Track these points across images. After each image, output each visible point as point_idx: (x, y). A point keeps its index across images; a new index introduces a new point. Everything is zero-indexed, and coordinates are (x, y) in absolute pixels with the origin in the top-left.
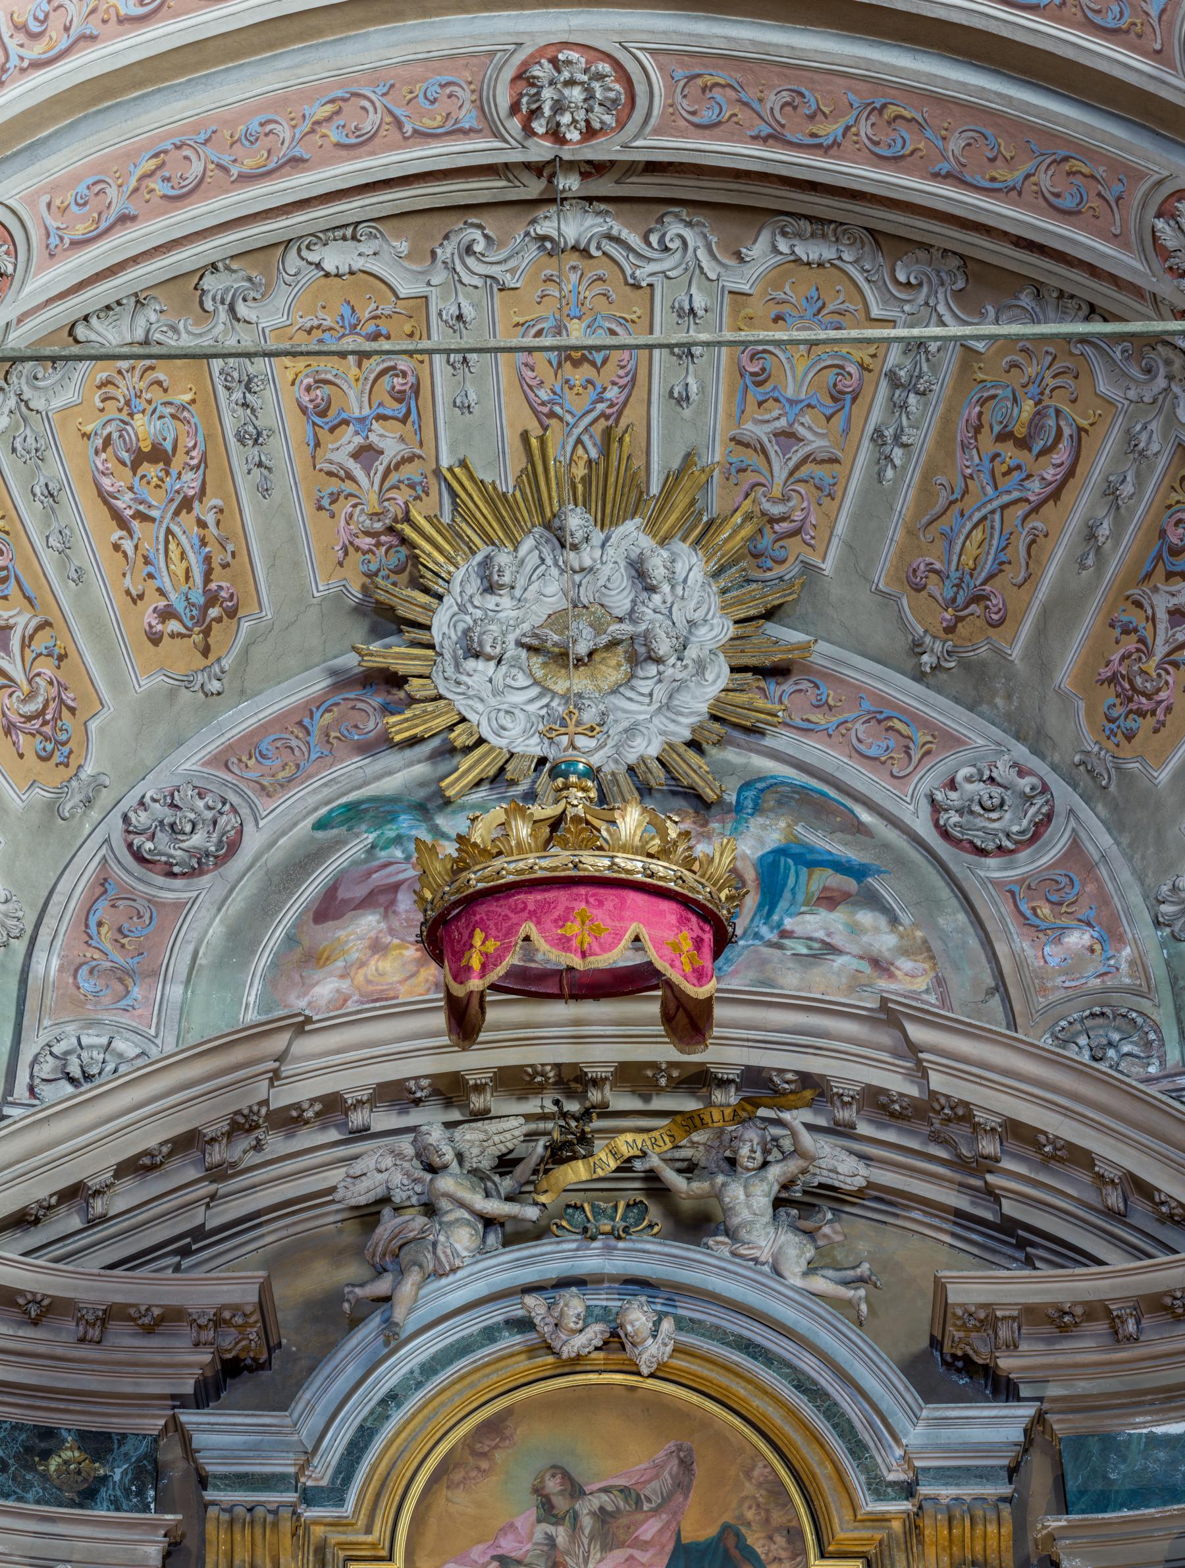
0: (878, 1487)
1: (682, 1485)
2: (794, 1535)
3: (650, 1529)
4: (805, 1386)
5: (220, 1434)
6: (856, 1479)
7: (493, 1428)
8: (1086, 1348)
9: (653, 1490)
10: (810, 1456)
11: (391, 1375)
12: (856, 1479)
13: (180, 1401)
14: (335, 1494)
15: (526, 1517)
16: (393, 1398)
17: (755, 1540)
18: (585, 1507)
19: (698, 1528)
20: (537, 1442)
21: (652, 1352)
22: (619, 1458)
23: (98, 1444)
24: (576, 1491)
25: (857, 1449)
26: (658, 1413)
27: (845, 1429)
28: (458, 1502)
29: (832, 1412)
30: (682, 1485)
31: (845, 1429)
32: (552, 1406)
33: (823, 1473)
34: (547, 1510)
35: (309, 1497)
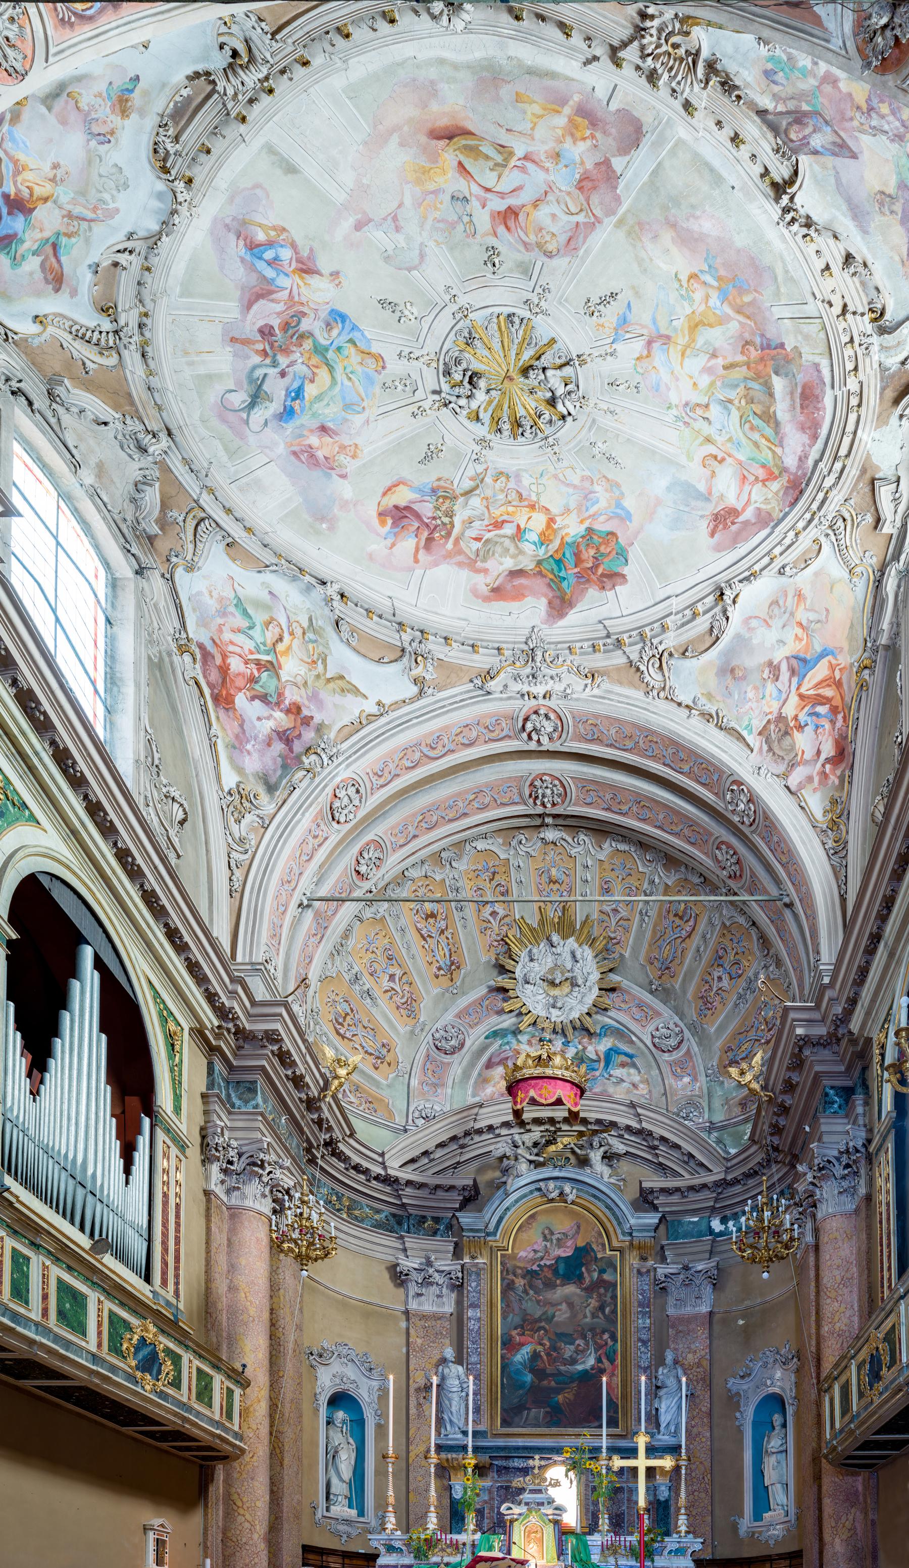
0: (624, 1233)
1: (577, 1232)
2: (603, 1245)
3: (569, 1243)
4: (608, 1207)
5: (466, 1219)
6: (619, 1231)
7: (532, 1217)
8: (675, 1198)
9: (570, 1233)
10: (608, 1225)
11: (507, 1203)
12: (619, 1231)
13: (457, 1210)
14: (494, 1233)
15: (540, 1239)
16: (508, 1209)
17: (594, 1246)
18: (554, 1238)
19: (581, 1243)
20: (542, 1220)
21: (571, 1198)
22: (562, 1225)
23: (437, 1220)
24: (552, 1233)
25: (620, 1224)
26: (573, 1213)
27: (617, 1219)
28: (524, 1236)
29: (614, 1214)
30: (577, 1232)
31: (617, 1219)
32: (546, 1211)
33: (611, 1230)
34: (545, 1238)
35: (488, 1234)
